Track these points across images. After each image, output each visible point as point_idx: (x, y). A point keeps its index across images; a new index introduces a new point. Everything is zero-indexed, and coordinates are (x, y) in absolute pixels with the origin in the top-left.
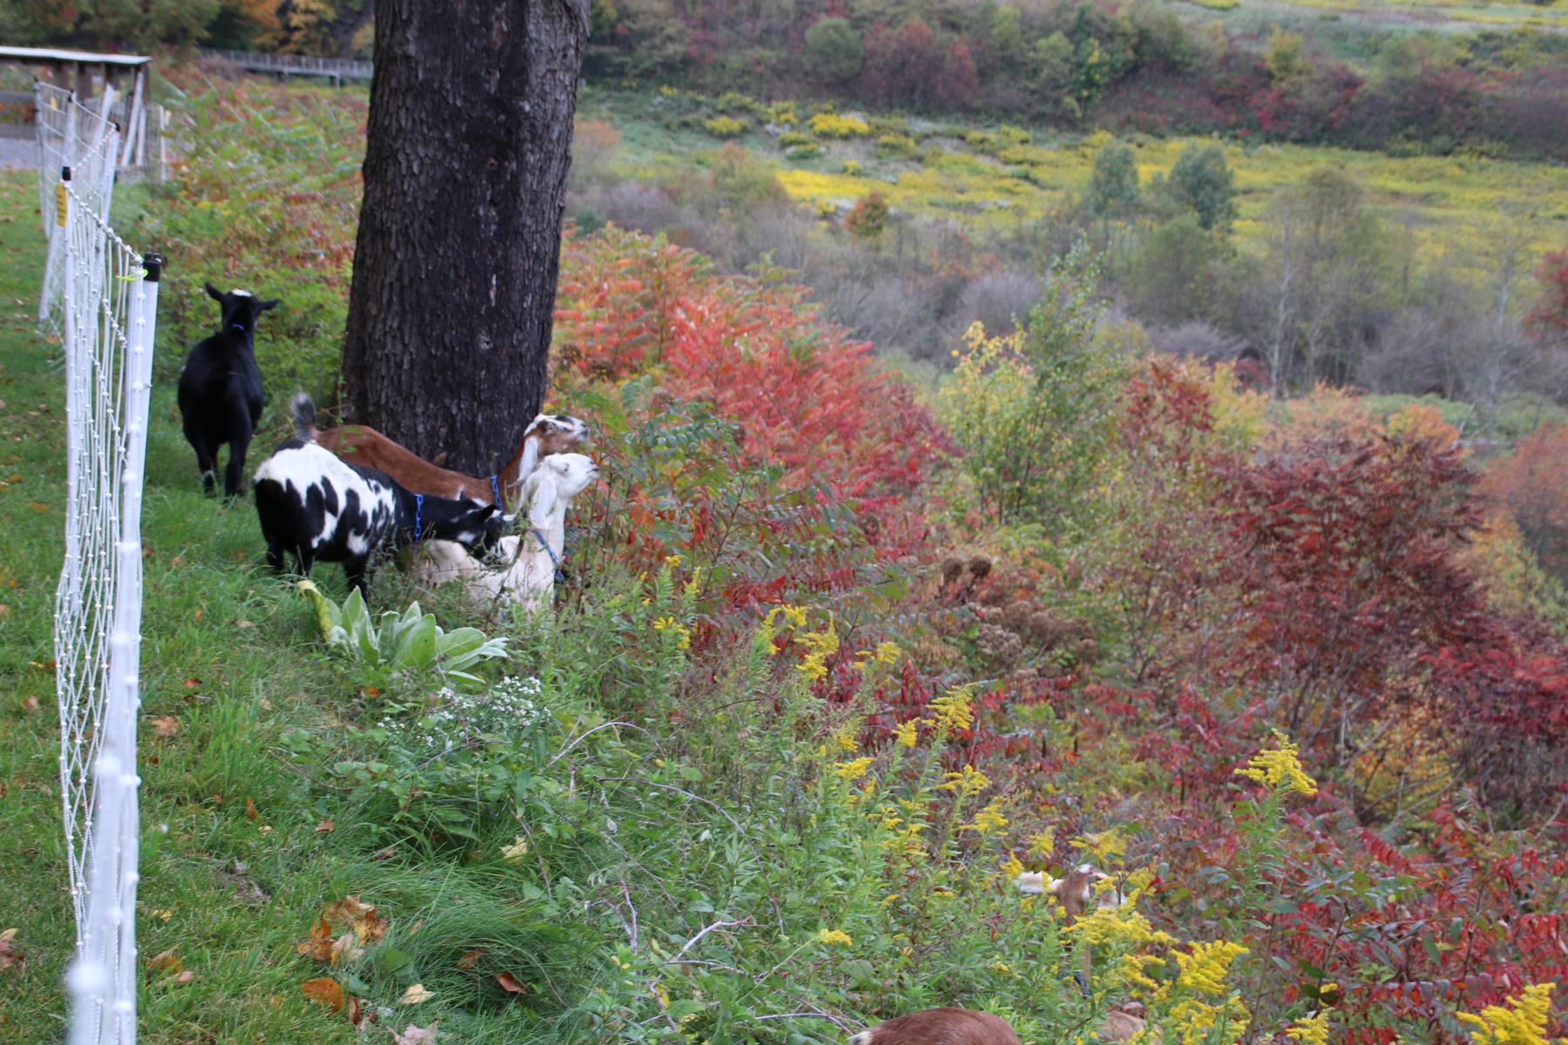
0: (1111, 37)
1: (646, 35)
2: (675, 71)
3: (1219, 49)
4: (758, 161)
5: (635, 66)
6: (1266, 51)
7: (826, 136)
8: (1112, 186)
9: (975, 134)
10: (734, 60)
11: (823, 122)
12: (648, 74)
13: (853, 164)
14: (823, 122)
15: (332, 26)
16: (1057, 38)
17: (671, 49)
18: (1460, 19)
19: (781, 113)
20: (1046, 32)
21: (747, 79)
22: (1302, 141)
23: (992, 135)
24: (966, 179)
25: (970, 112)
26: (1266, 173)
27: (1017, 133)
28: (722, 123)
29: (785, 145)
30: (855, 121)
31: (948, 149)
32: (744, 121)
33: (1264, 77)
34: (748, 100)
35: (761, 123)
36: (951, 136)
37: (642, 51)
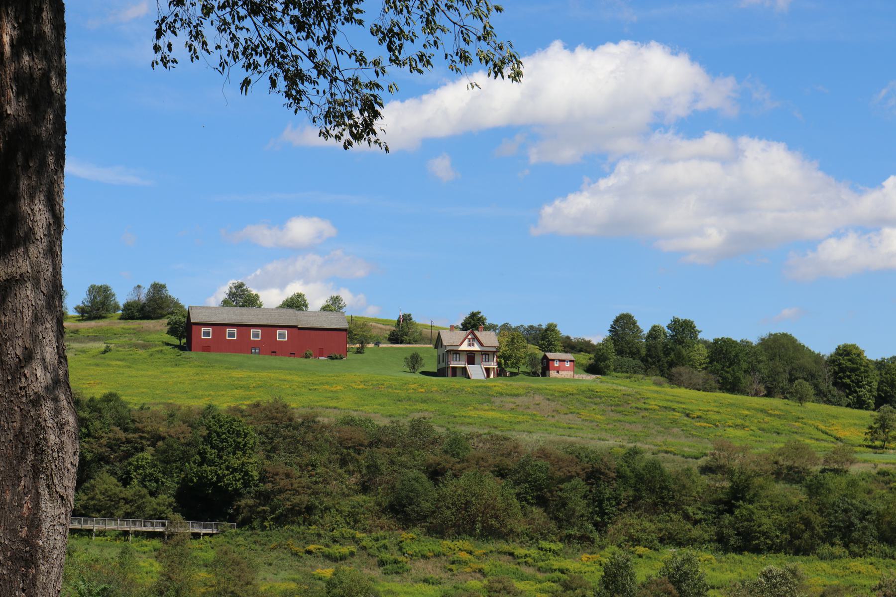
5: (272, 512)
12: (280, 521)
17: (296, 499)
18: (865, 461)
28: (337, 549)
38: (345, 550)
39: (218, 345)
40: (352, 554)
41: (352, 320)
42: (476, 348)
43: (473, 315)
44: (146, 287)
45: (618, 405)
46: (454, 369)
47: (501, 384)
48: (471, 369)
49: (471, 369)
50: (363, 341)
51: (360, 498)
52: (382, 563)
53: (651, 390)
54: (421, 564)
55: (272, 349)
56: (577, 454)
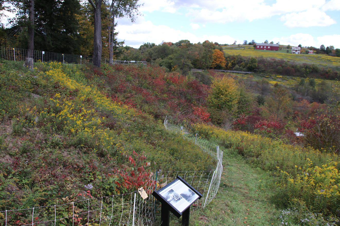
0: (310, 68)
1: (260, 68)
2: (263, 71)
3: (322, 70)
4: (266, 80)
6: (327, 70)
7: (278, 78)
8: (302, 83)
9: (293, 78)
10: (269, 70)
11: (277, 76)
12: (260, 72)
13: (280, 80)
14: (277, 76)
15: (231, 68)
16: (304, 69)
19: (273, 76)
20: (303, 68)
21: (271, 72)
22: (331, 79)
23: (295, 78)
24: (292, 82)
25: (294, 76)
26: (318, 81)
27: (298, 78)
28: (267, 76)
29: (273, 78)
30: (281, 76)
31: (290, 80)
32: (269, 76)
33: (327, 73)
34: (270, 74)
35: (271, 76)
36: (291, 78)
37: (260, 69)
38: (268, 76)
39: (260, 48)
40: (269, 77)
41: (280, 45)
42: (297, 49)
43: (300, 45)
44: (252, 41)
45: (318, 58)
46: (294, 53)
47: (300, 55)
48: (296, 52)
49: (296, 52)
50: (281, 48)
51: (272, 70)
52: (273, 78)
53: (324, 56)
54: (278, 79)
55: (267, 49)
56: (304, 64)
